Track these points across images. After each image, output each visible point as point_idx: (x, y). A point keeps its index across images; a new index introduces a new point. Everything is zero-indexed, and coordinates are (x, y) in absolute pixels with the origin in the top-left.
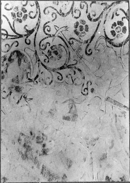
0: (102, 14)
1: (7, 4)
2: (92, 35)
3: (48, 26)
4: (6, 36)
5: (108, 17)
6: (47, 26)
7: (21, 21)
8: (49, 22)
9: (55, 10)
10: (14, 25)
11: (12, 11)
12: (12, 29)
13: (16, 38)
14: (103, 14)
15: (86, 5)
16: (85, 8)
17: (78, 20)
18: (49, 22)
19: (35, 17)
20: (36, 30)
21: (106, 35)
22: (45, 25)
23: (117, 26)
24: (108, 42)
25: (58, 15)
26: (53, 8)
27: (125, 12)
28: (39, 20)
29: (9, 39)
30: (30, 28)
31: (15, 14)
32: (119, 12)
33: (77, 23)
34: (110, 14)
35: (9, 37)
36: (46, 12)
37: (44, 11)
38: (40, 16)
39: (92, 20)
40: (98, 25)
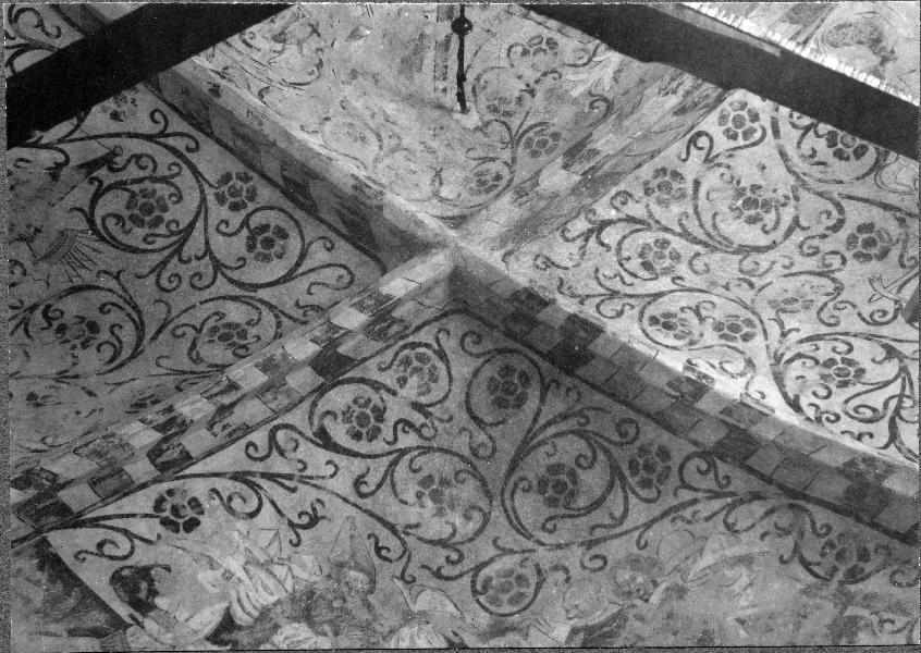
0: (821, 194)
2: (881, 211)
5: (829, 177)
6: (873, 319)
8: (859, 315)
11: (833, 386)
12: (883, 387)
14: (821, 190)
15: (810, 242)
16: (816, 242)
17: (848, 255)
18: (859, 315)
20: (885, 341)
21: (871, 170)
22: (868, 323)
23: (840, 146)
24: (885, 160)
25: (839, 299)
27: (804, 135)
28: (855, 336)
30: (881, 354)
31: (840, 382)
32: (806, 148)
33: (857, 256)
34: (816, 171)
36: (832, 321)
37: (830, 325)
38: (847, 334)
39: (841, 217)
40: (850, 197)
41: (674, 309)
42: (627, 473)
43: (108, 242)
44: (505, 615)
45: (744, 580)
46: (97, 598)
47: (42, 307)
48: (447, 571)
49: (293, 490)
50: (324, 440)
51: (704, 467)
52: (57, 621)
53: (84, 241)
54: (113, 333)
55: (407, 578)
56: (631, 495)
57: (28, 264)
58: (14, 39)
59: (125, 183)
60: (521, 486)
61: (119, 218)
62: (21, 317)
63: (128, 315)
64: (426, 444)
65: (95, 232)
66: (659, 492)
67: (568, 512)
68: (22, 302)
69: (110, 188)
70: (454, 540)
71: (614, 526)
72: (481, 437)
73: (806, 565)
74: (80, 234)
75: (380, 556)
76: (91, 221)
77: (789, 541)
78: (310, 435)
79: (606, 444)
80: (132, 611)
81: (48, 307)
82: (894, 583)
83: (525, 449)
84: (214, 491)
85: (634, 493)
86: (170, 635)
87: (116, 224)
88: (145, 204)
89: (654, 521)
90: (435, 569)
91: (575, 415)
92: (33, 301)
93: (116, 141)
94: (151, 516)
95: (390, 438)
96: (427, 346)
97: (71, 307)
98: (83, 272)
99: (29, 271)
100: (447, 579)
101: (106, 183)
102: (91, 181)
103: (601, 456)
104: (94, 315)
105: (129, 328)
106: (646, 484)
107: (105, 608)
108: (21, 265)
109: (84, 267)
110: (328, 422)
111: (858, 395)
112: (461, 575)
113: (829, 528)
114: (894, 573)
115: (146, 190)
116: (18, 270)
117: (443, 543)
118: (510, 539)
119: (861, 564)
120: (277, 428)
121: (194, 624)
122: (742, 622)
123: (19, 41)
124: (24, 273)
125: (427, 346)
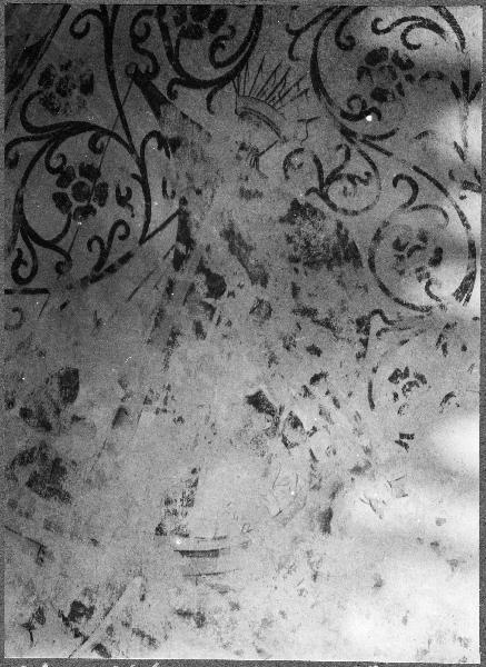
43: (249, 54)
47: (345, 121)
53: (250, 84)
54: (387, 30)
57: (287, 148)
58: (20, 251)
59: (169, 49)
61: (216, 45)
62: (364, 147)
65: (237, 70)
68: (340, 147)
69: (178, 68)
74: (241, 93)
76: (220, 83)
81: (344, 115)
87: (223, 47)
88: (194, 16)
92: (337, 132)
93: (118, 77)
97: (342, 85)
98: (291, 80)
99: (297, 145)
101: (173, 75)
102: (173, 95)
104: (356, 58)
108: (290, 155)
109: (284, 77)
115: (175, 19)
116: (296, 160)
123: (20, 243)
124: (299, 151)
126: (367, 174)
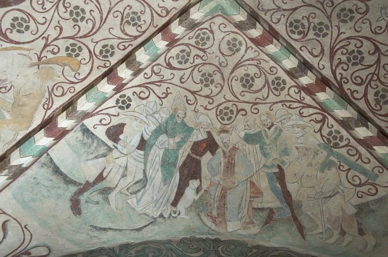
1: (342, 68)
3: (375, 29)
4: (375, 76)
7: (363, 58)
9: (359, 20)
10: (365, 66)
11: (350, 65)
13: (380, 65)
19: (362, 43)
22: (373, 32)
25: (365, 17)
26: (357, 22)
29: (378, 73)
35: (376, 73)
41: (300, 18)
42: (271, 84)
44: (225, 124)
45: (301, 134)
46: (103, 142)
48: (209, 107)
49: (160, 86)
50: (169, 66)
51: (297, 91)
52: (92, 153)
54: (91, 14)
55: (196, 111)
56: (270, 92)
60: (234, 78)
63: (96, 5)
64: (204, 62)
66: (280, 94)
67: (249, 91)
70: (211, 95)
71: (263, 100)
72: (223, 59)
73: (322, 136)
75: (188, 103)
77: (319, 125)
78: (165, 65)
79: (265, 72)
80: (113, 143)
82: (348, 153)
83: (236, 67)
84: (134, 92)
85: (272, 91)
86: (126, 150)
89: (277, 103)
90: (205, 106)
91: (256, 60)
94: (115, 107)
95: (192, 62)
96: (206, 29)
100: (208, 110)
103: (263, 76)
105: (97, 11)
106: (276, 89)
107: (106, 145)
110: (171, 60)
111: (359, 70)
112: (213, 109)
113: (333, 126)
114: (349, 150)
117: (207, 97)
118: (229, 96)
119: (339, 142)
120: (154, 66)
121: (132, 143)
122: (297, 148)
125: (206, 29)
126: (45, 9)
